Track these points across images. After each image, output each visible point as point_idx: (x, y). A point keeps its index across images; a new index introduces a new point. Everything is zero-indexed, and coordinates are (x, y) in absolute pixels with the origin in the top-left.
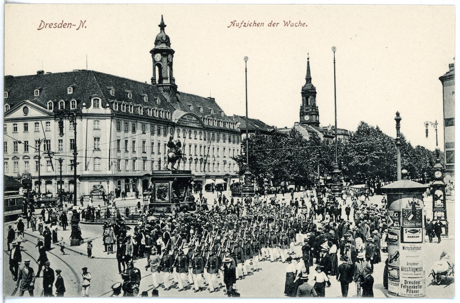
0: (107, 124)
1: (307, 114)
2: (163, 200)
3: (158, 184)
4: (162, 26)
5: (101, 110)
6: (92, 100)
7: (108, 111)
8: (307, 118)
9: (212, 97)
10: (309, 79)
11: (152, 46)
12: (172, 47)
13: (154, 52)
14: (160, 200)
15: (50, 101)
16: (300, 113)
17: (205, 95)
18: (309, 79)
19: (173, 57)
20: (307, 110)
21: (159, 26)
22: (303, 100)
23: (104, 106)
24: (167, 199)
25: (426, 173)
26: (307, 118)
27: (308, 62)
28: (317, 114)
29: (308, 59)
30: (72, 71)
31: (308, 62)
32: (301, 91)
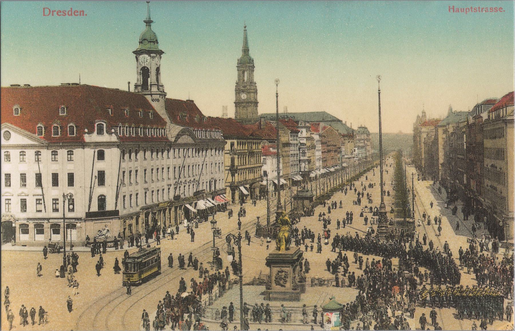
0: (113, 154)
1: (243, 92)
2: (282, 286)
3: (275, 270)
4: (148, 22)
5: (105, 138)
6: (96, 125)
7: (114, 138)
8: (244, 96)
9: (191, 99)
10: (246, 50)
11: (137, 46)
12: (161, 47)
13: (138, 53)
14: (278, 287)
15: (39, 125)
16: (236, 90)
17: (184, 98)
18: (246, 50)
19: (161, 58)
20: (245, 87)
21: (145, 22)
22: (239, 76)
23: (109, 133)
24: (288, 285)
25: (485, 218)
26: (244, 96)
27: (245, 30)
28: (256, 92)
29: (245, 27)
30: (60, 85)
31: (245, 30)
32: (237, 65)
